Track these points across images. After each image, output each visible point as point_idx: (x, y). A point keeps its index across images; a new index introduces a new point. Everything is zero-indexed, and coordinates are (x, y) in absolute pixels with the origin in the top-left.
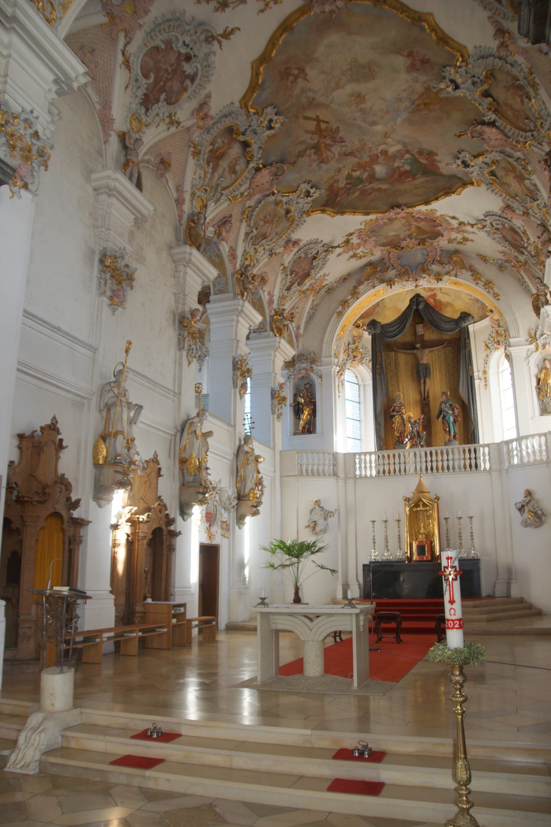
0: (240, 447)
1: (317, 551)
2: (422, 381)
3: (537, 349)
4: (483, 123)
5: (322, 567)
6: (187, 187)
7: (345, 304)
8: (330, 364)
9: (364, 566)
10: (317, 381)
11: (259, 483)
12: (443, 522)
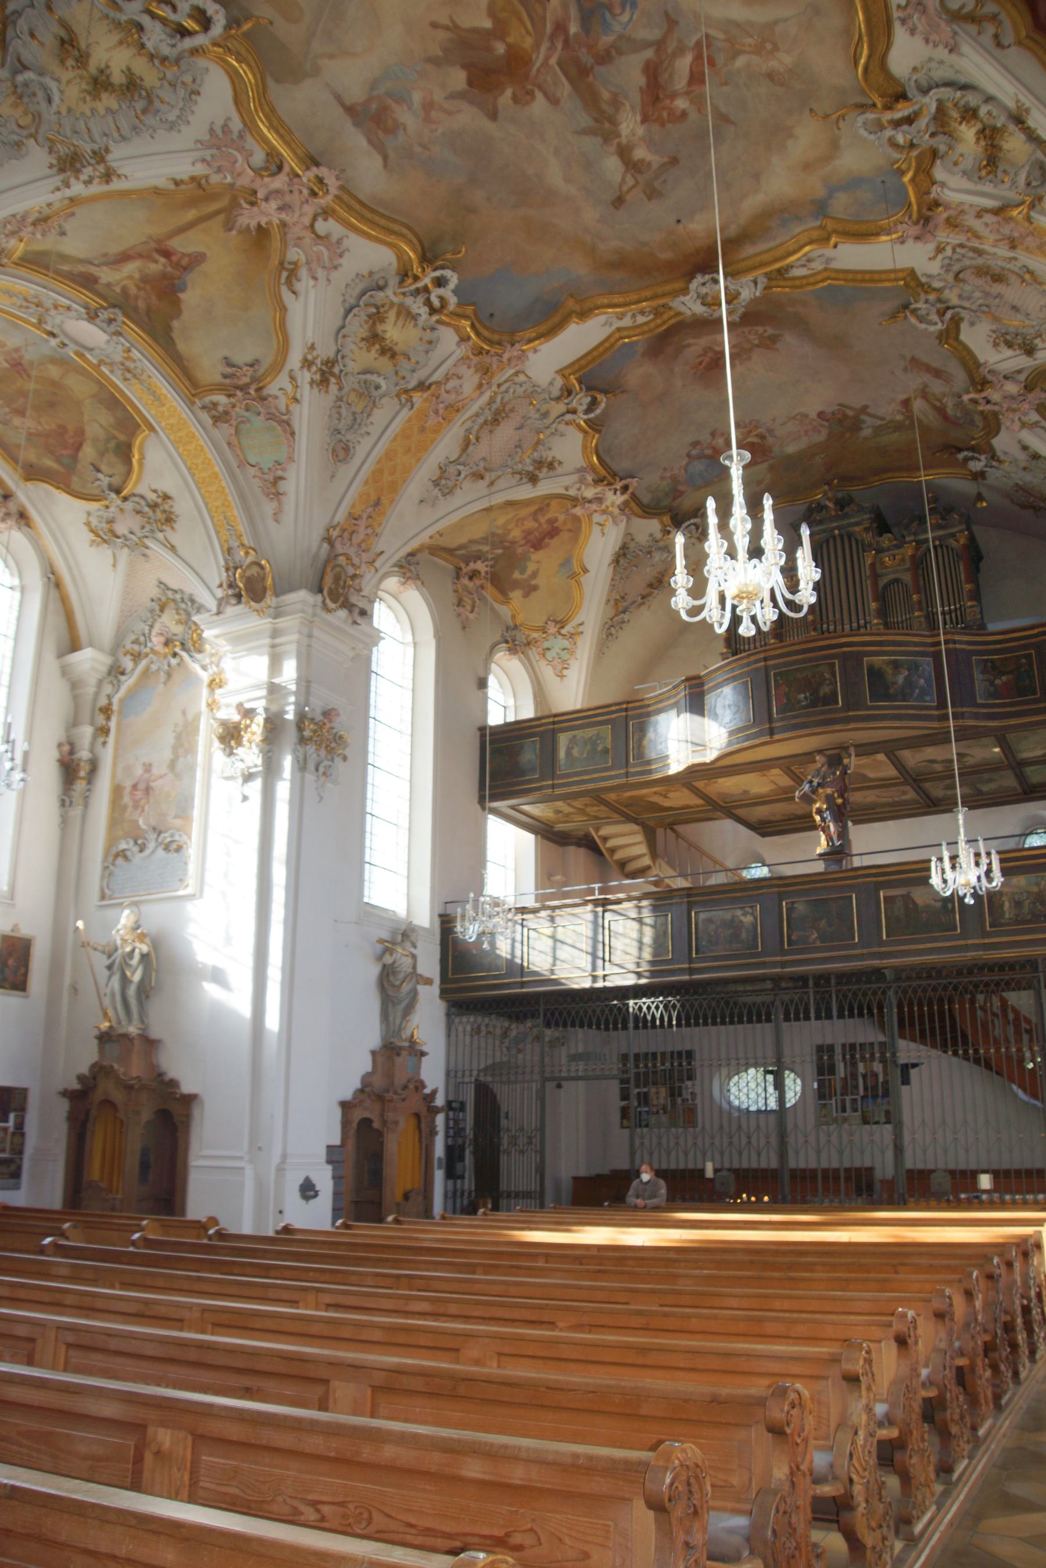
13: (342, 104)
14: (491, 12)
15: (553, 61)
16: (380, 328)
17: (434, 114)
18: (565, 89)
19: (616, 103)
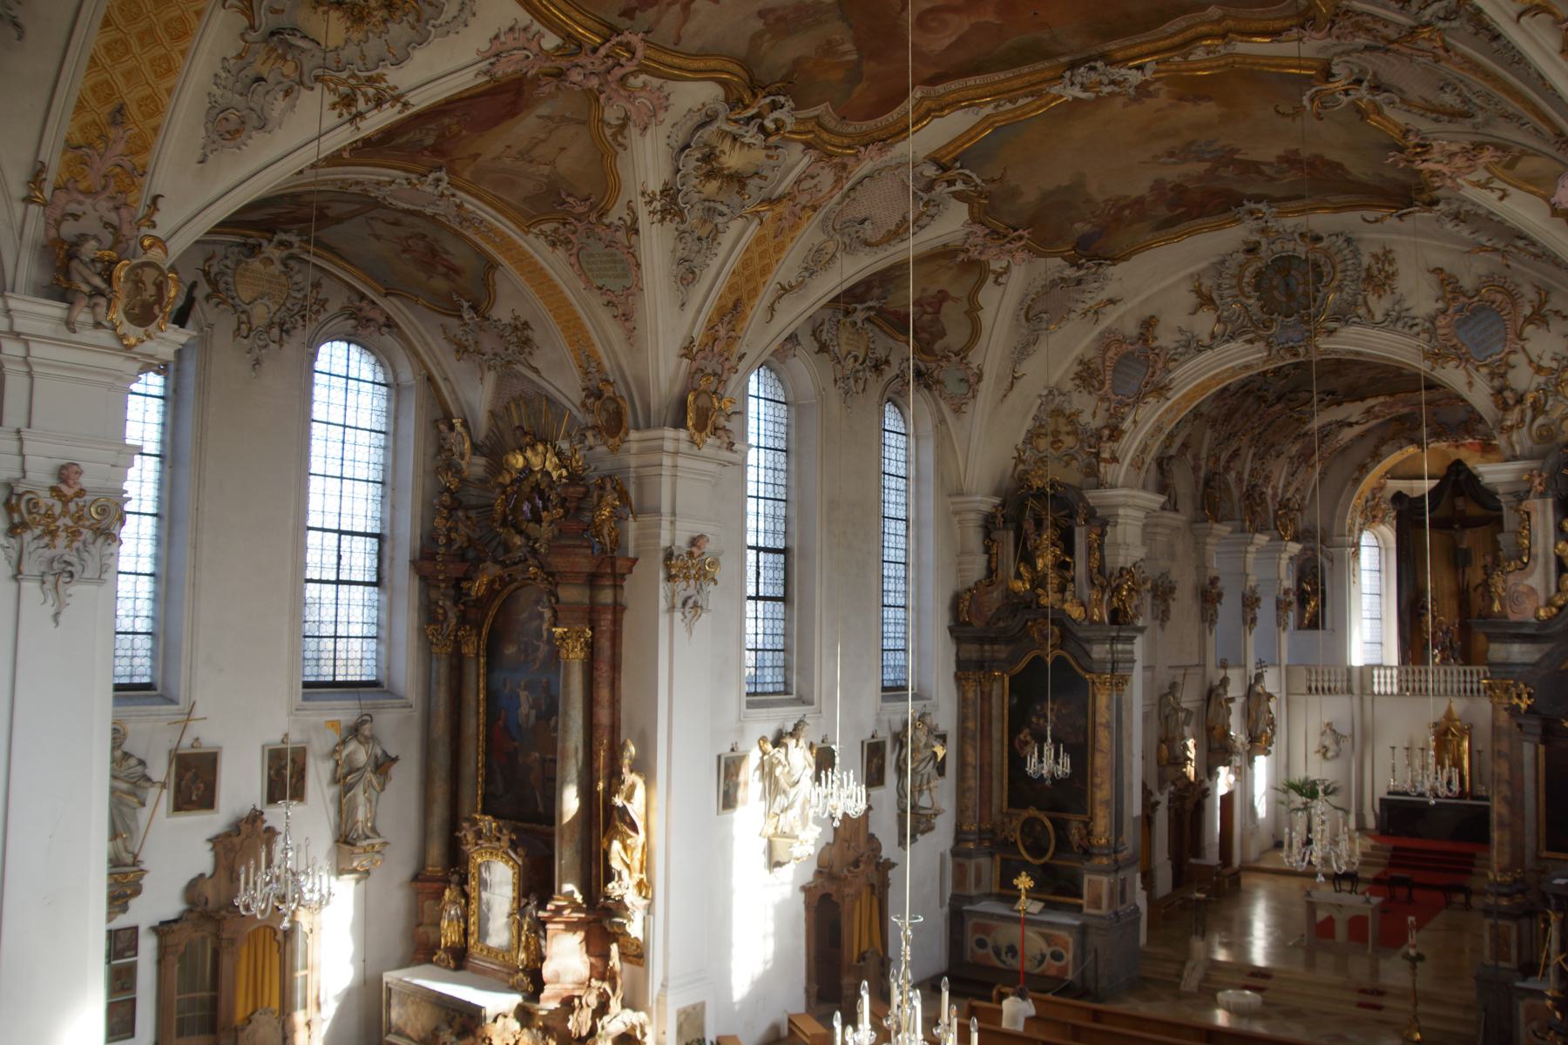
0: (1250, 686)
1: (1331, 793)
5: (1336, 808)
6: (1204, 455)
7: (1363, 469)
8: (1343, 546)
9: (1382, 801)
10: (1327, 565)
11: (1271, 723)
12: (1475, 755)
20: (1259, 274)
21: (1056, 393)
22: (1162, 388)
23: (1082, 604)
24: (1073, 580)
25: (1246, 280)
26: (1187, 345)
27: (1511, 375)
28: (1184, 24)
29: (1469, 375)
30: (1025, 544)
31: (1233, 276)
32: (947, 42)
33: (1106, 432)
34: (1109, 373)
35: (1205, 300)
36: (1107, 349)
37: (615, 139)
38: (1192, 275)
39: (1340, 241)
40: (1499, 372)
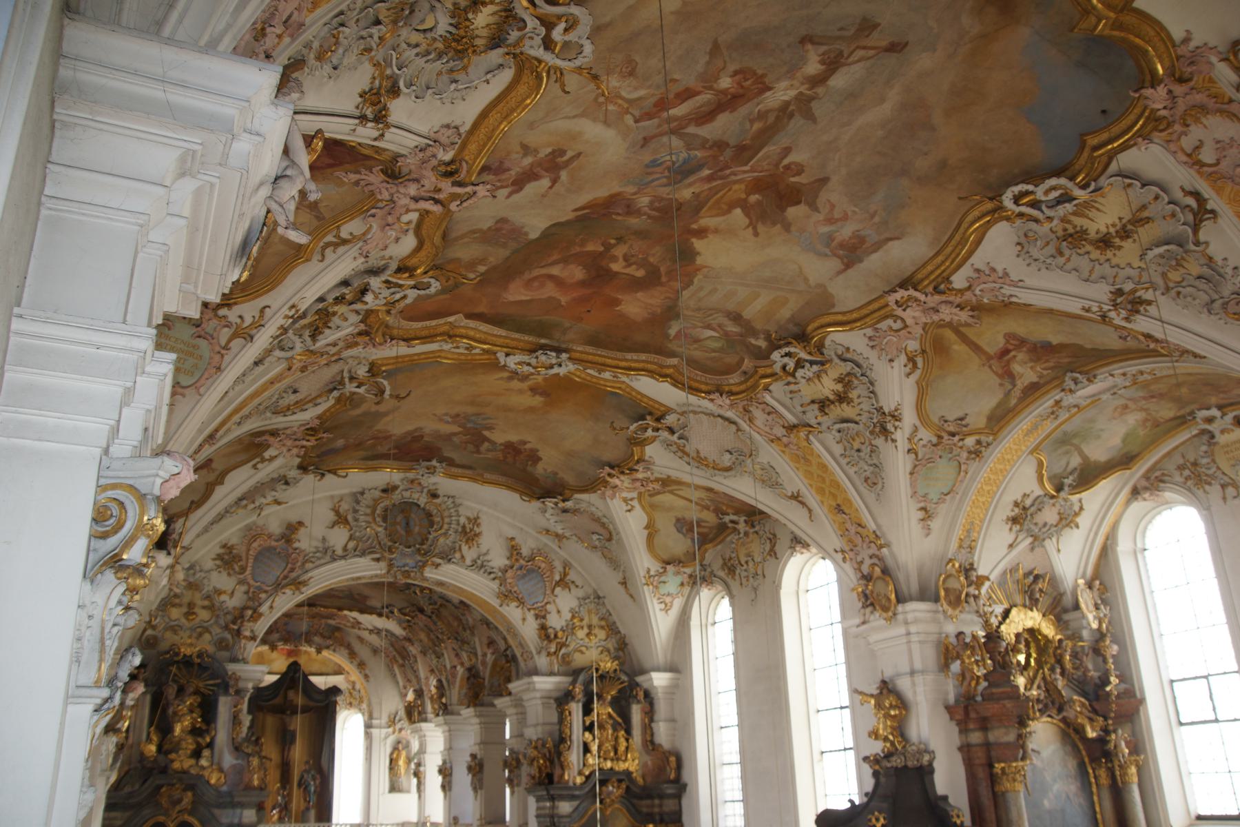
2: (287, 748)
3: (394, 732)
4: (422, 611)
13: (845, 270)
14: (729, 211)
15: (747, 168)
16: (1092, 234)
17: (836, 215)
18: (771, 149)
19: (762, 116)
20: (386, 510)
21: (198, 568)
22: (300, 583)
23: (221, 770)
24: (210, 745)
25: (378, 512)
26: (326, 550)
27: (548, 616)
28: (644, 358)
29: (524, 613)
30: (164, 710)
31: (368, 507)
32: (524, 298)
33: (249, 612)
34: (251, 561)
35: (341, 519)
36: (254, 538)
37: (324, 248)
38: (332, 497)
39: (450, 501)
40: (541, 616)
